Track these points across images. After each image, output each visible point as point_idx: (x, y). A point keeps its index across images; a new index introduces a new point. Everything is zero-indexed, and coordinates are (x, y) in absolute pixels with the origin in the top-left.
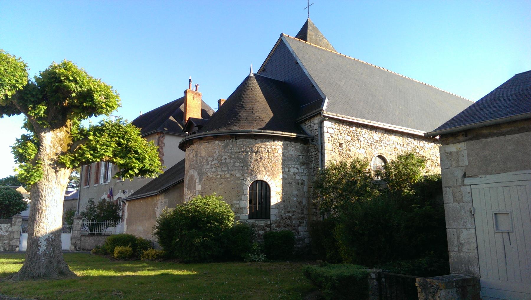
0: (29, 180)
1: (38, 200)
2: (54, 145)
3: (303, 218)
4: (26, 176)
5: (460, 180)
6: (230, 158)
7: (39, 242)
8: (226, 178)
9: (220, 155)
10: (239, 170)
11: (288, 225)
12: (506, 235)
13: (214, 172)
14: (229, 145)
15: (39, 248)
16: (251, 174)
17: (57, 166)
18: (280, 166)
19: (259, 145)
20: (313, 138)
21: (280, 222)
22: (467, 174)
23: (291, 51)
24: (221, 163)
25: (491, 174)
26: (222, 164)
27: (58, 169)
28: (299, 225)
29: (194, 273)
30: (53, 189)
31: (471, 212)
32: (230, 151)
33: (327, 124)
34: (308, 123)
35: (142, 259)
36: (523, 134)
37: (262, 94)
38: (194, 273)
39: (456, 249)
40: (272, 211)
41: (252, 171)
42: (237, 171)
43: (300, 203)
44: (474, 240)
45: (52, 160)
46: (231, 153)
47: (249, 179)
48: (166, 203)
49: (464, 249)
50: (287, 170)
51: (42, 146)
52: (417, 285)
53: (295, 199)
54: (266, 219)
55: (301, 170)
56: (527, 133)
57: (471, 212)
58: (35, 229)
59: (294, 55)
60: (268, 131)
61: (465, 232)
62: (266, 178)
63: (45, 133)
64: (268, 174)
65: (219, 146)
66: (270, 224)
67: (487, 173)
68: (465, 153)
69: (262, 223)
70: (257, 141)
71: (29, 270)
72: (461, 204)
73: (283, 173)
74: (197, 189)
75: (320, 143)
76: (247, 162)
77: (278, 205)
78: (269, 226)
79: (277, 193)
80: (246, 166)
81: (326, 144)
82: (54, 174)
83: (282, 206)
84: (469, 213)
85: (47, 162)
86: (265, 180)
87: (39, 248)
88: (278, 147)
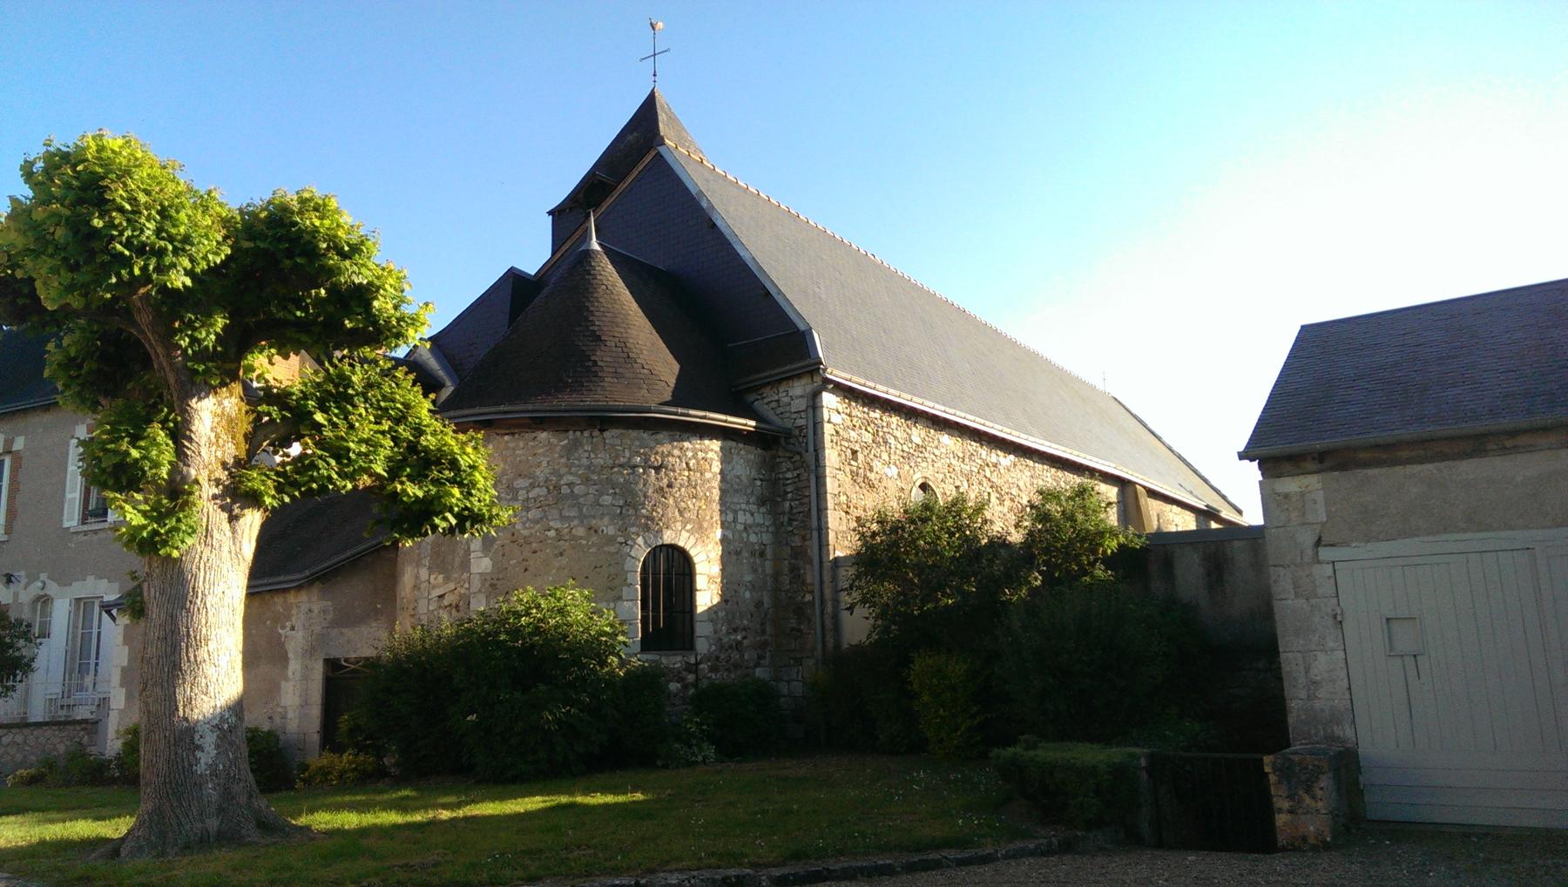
0: (165, 543)
1: (183, 607)
2: (217, 437)
3: (763, 645)
4: (155, 533)
5: (1309, 552)
6: (586, 481)
7: (197, 737)
8: (575, 538)
9: (555, 472)
10: (613, 518)
11: (736, 666)
12: (1410, 661)
13: (537, 522)
14: (581, 445)
15: (199, 754)
16: (647, 528)
17: (233, 502)
18: (716, 507)
19: (665, 448)
20: (788, 434)
21: (717, 658)
22: (1325, 540)
23: (694, 192)
24: (557, 495)
25: (1378, 540)
26: (560, 498)
27: (237, 511)
28: (757, 665)
29: (639, 796)
30: (225, 571)
31: (1335, 617)
32: (585, 462)
33: (829, 400)
34: (770, 394)
35: (299, 785)
36: (1442, 465)
37: (634, 305)
38: (650, 796)
39: (1303, 694)
40: (702, 629)
41: (648, 518)
42: (606, 520)
43: (759, 604)
44: (1343, 674)
45: (218, 482)
46: (588, 467)
47: (640, 540)
48: (325, 611)
49: (1322, 693)
50: (730, 517)
51: (190, 440)
52: (1267, 769)
53: (747, 595)
54: (683, 649)
55: (759, 519)
56: (1450, 463)
57: (1335, 617)
58: (180, 698)
59: (704, 204)
60: (692, 412)
61: (1322, 658)
62: (684, 540)
63: (200, 399)
64: (689, 527)
65: (551, 447)
66: (697, 664)
67: (1368, 538)
68: (1320, 496)
69: (673, 661)
70: (660, 436)
71: (174, 822)
72: (1313, 601)
73: (723, 526)
74: (474, 569)
75: (811, 449)
76: (634, 494)
77: (712, 610)
78: (693, 668)
79: (711, 579)
80: (632, 508)
81: (827, 452)
82: (226, 526)
83: (722, 614)
84: (1330, 621)
85: (206, 492)
86: (681, 544)
87: (199, 754)
88: (710, 455)
